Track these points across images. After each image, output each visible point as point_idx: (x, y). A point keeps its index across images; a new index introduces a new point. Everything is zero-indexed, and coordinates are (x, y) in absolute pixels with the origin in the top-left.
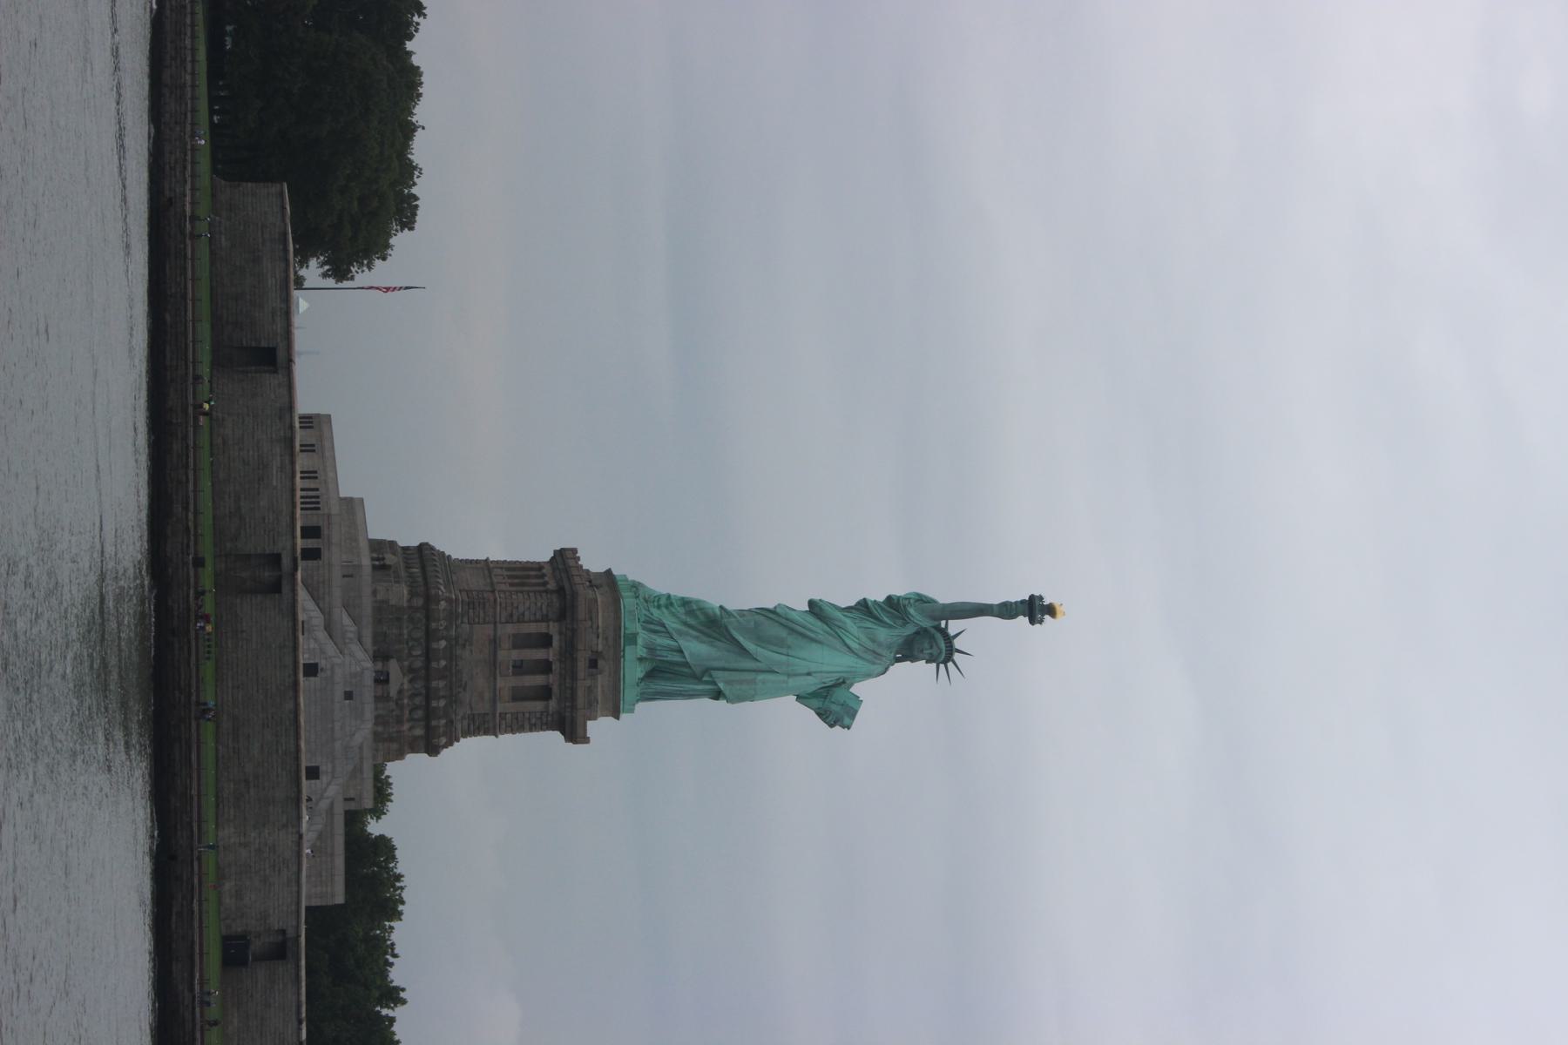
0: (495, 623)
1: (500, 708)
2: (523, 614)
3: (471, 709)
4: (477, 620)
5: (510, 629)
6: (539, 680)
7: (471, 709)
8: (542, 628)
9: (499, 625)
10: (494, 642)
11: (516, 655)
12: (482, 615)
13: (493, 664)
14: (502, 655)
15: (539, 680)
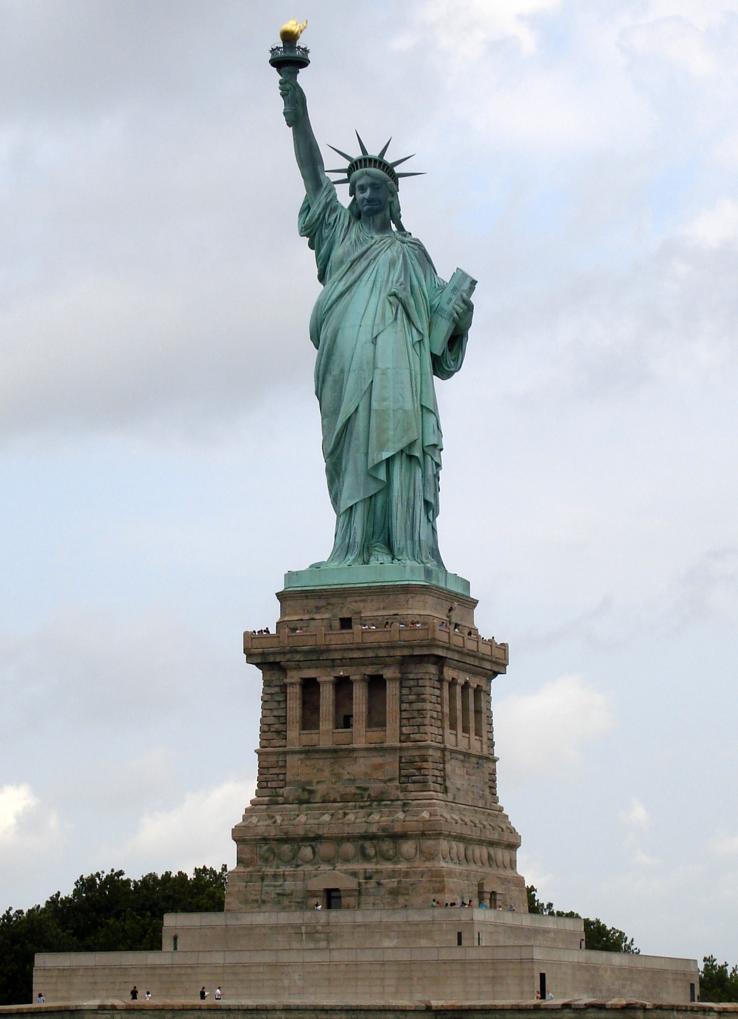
0: (285, 753)
1: (392, 741)
2: (278, 717)
3: (391, 780)
4: (281, 777)
5: (293, 732)
6: (359, 693)
7: (391, 780)
8: (294, 692)
9: (289, 748)
10: (309, 752)
11: (326, 724)
12: (277, 771)
13: (336, 753)
14: (325, 742)
15: (359, 693)
